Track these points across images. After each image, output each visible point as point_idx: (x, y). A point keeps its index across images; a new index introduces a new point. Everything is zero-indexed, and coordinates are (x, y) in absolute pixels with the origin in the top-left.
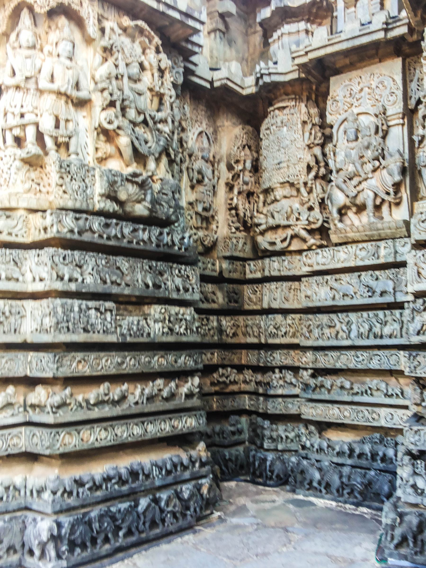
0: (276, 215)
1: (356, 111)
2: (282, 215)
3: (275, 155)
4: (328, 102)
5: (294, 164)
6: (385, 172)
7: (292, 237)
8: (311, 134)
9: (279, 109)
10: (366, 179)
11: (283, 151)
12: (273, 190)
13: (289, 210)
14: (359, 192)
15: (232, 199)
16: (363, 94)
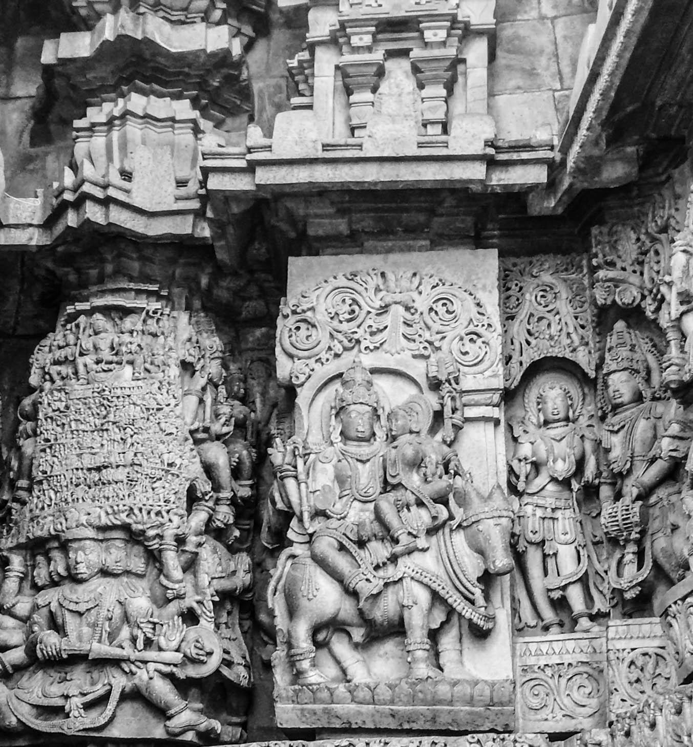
0: (71, 623)
1: (369, 360)
2: (94, 626)
3: (87, 440)
4: (280, 321)
5: (154, 479)
6: (459, 539)
7: (125, 697)
8: (201, 401)
9: (106, 310)
10: (409, 552)
11: (116, 434)
12: (64, 546)
13: (118, 612)
14: (386, 585)
16: (387, 319)
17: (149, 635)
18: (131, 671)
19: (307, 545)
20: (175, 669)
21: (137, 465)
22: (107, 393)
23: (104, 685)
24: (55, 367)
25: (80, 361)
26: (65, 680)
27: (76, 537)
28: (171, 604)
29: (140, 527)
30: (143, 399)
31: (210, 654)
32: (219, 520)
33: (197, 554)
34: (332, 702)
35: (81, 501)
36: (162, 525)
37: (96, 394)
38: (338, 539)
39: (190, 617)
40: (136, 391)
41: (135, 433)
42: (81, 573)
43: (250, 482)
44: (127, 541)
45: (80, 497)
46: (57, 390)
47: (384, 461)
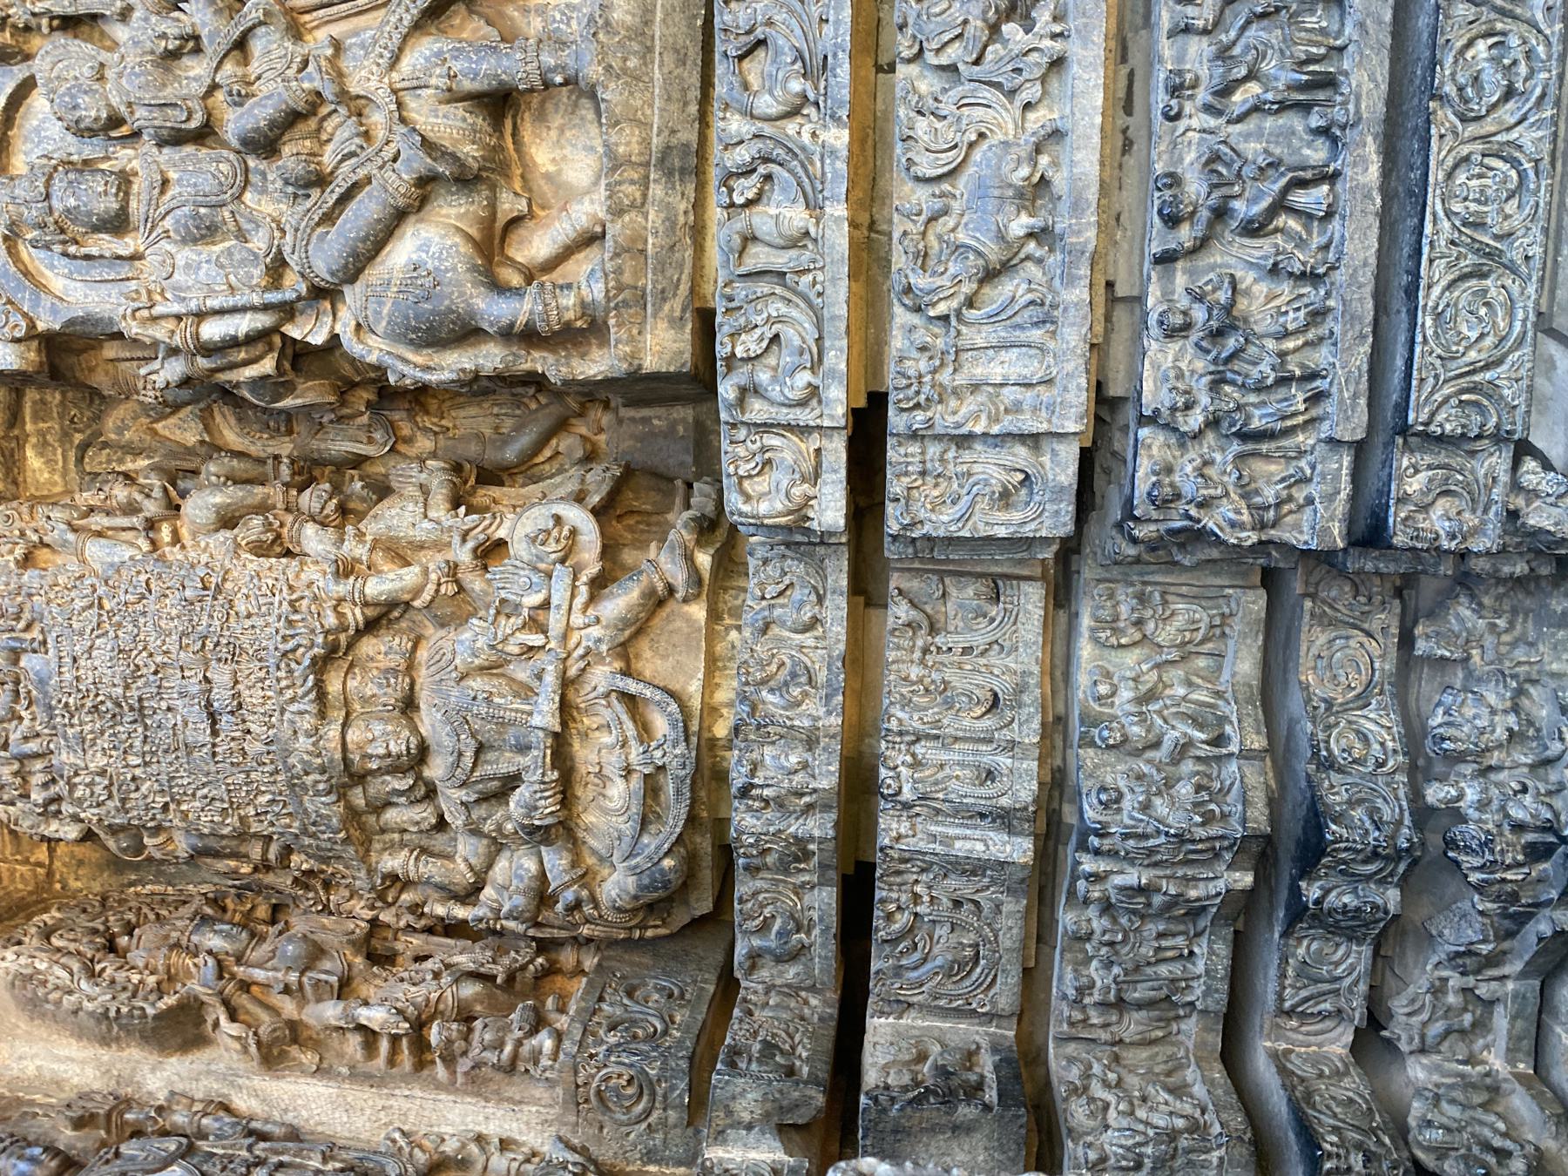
13: (477, 684)
15: (369, 1036)
17: (520, 621)
18: (582, 657)
19: (340, 306)
20: (584, 579)
21: (204, 645)
22: (71, 701)
23: (609, 705)
24: (33, 796)
25: (14, 749)
26: (599, 774)
27: (338, 756)
28: (468, 586)
29: (320, 639)
30: (81, 634)
31: (558, 520)
32: (323, 508)
33: (375, 541)
34: (643, 252)
35: (273, 748)
36: (315, 598)
37: (75, 721)
38: (312, 223)
39: (491, 551)
40: (66, 649)
41: (145, 648)
42: (408, 749)
43: (270, 461)
44: (352, 666)
45: (265, 748)
46: (71, 792)
47: (161, 144)
